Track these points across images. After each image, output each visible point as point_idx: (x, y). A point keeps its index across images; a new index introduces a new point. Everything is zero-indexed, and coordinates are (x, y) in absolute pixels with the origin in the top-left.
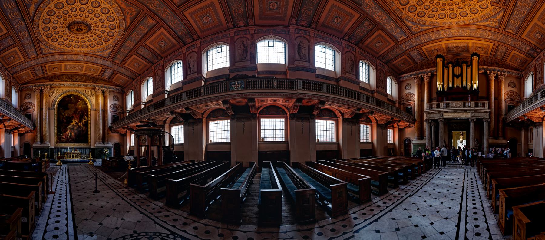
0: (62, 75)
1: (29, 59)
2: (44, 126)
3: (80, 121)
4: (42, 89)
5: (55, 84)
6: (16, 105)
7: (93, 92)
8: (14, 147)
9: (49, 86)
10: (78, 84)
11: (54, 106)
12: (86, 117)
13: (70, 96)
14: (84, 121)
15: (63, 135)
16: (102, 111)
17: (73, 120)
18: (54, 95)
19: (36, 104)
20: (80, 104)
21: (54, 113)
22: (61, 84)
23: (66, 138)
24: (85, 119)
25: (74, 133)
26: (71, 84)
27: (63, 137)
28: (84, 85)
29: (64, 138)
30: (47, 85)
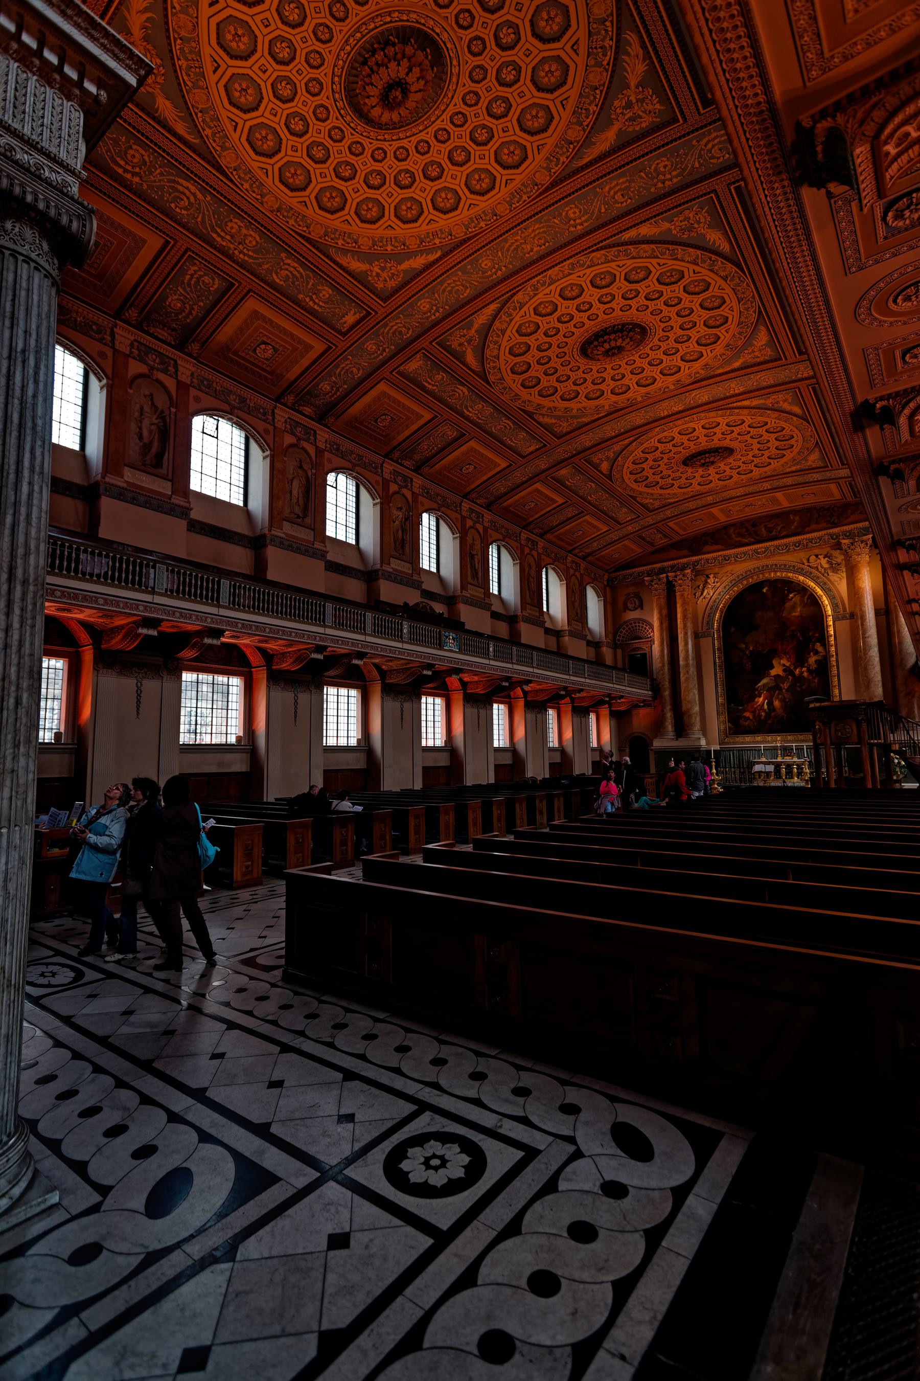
0: (726, 528)
2: (683, 686)
3: (800, 660)
4: (671, 579)
5: (707, 560)
6: (600, 633)
7: (839, 557)
8: (600, 749)
9: (689, 571)
10: (777, 547)
11: (710, 624)
12: (819, 647)
13: (761, 584)
14: (812, 659)
15: (744, 710)
16: (877, 613)
17: (774, 662)
18: (708, 592)
19: (656, 624)
20: (793, 608)
21: (712, 645)
22: (726, 558)
23: (754, 716)
24: (816, 653)
25: (783, 701)
26: (756, 551)
27: (747, 714)
28: (799, 542)
29: (748, 718)
30: (683, 568)
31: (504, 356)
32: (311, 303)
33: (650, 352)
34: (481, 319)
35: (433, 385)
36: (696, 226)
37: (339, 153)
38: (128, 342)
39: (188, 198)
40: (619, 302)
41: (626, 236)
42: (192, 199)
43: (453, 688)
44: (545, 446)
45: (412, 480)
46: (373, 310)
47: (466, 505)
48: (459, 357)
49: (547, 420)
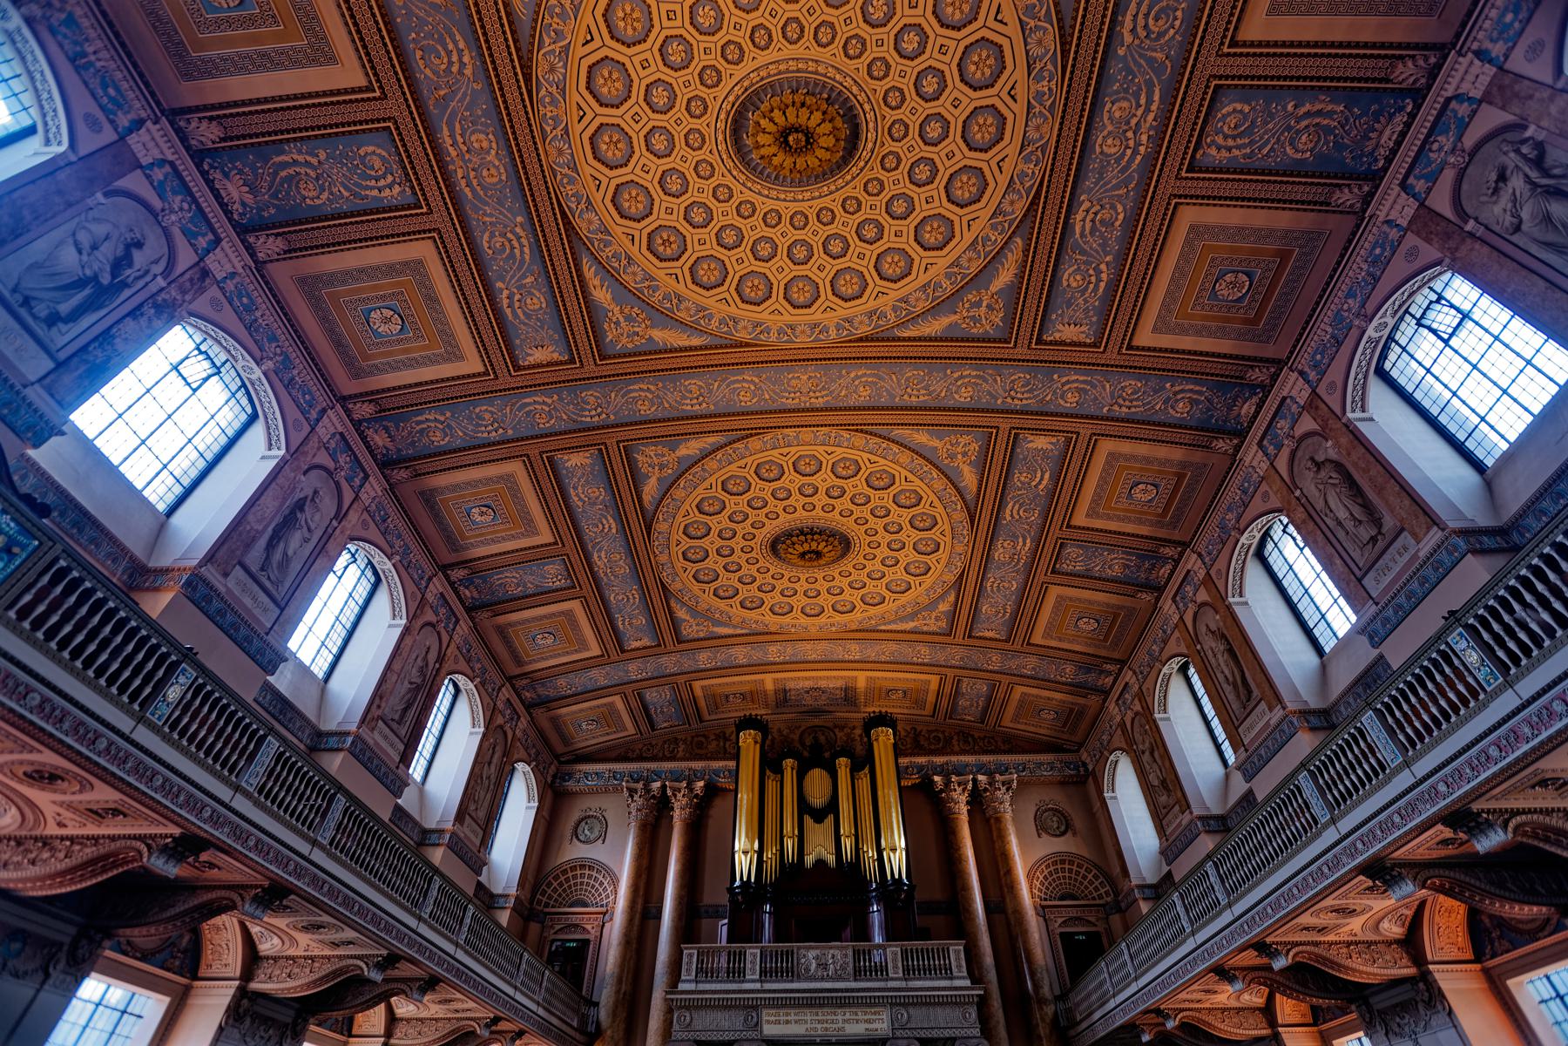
1: (623, 651)
31: (689, 505)
32: (505, 302)
33: (837, 576)
34: (691, 448)
35: (580, 499)
36: (960, 456)
37: (683, 161)
38: (156, 154)
39: (450, 63)
40: (844, 504)
41: (897, 432)
42: (455, 69)
43: (363, 1031)
44: (659, 645)
45: (457, 621)
46: (581, 361)
47: (506, 693)
48: (636, 480)
49: (681, 614)
